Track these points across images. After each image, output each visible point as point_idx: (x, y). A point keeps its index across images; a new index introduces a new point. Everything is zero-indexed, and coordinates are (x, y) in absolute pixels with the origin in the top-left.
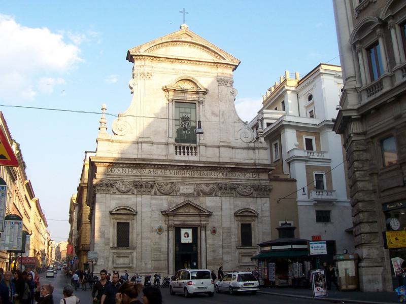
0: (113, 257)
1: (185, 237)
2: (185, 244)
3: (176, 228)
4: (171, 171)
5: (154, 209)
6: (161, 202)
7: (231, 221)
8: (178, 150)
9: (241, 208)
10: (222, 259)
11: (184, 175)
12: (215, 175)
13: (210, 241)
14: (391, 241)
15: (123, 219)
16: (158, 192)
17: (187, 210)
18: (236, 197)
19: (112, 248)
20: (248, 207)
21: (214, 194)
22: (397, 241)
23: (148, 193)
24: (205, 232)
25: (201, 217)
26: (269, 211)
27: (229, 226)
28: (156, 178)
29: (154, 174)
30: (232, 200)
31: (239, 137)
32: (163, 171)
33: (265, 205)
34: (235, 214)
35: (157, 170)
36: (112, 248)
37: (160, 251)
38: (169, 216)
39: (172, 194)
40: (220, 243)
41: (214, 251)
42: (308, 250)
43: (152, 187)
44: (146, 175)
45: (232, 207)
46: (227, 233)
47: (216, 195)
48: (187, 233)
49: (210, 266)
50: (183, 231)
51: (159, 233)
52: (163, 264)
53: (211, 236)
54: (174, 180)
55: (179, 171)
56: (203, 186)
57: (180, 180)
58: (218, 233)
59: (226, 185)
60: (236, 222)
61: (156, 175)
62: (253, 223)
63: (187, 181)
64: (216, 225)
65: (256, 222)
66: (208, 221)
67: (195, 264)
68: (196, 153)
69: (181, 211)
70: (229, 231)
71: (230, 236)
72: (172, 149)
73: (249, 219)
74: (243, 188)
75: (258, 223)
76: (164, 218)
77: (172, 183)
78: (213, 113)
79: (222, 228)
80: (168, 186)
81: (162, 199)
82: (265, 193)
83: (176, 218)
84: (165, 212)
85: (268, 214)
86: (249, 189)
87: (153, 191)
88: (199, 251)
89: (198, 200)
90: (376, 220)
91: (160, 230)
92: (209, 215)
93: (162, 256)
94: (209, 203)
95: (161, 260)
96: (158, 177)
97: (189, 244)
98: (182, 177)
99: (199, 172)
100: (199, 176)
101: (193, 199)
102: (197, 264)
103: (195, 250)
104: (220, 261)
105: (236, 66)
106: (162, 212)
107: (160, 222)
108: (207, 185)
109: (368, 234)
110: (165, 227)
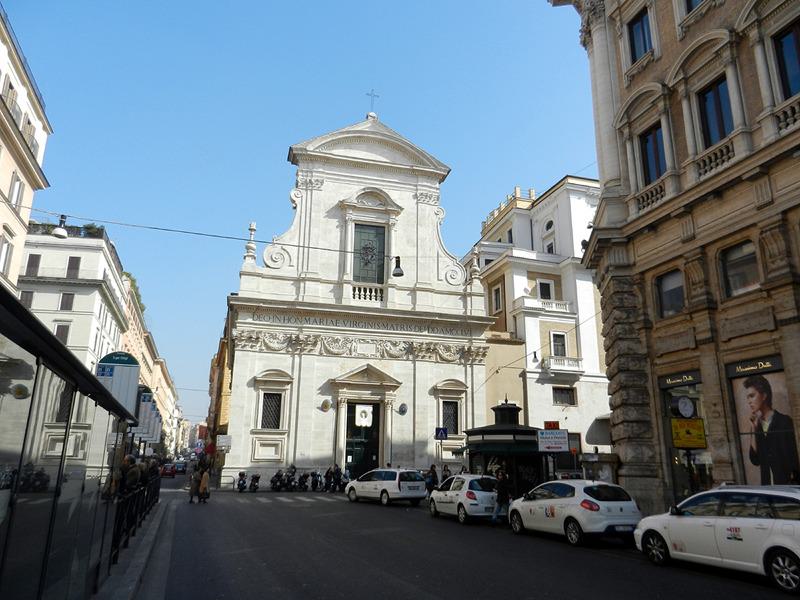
0: (253, 444)
8: (357, 292)
15: (273, 389)
19: (253, 432)
31: (442, 277)
36: (253, 432)
42: (535, 444)
43: (315, 344)
48: (364, 412)
50: (359, 409)
56: (389, 344)
67: (374, 458)
68: (382, 297)
72: (348, 290)
78: (408, 242)
91: (324, 407)
94: (395, 369)
102: (377, 458)
105: (444, 177)
108: (395, 344)
109: (635, 424)
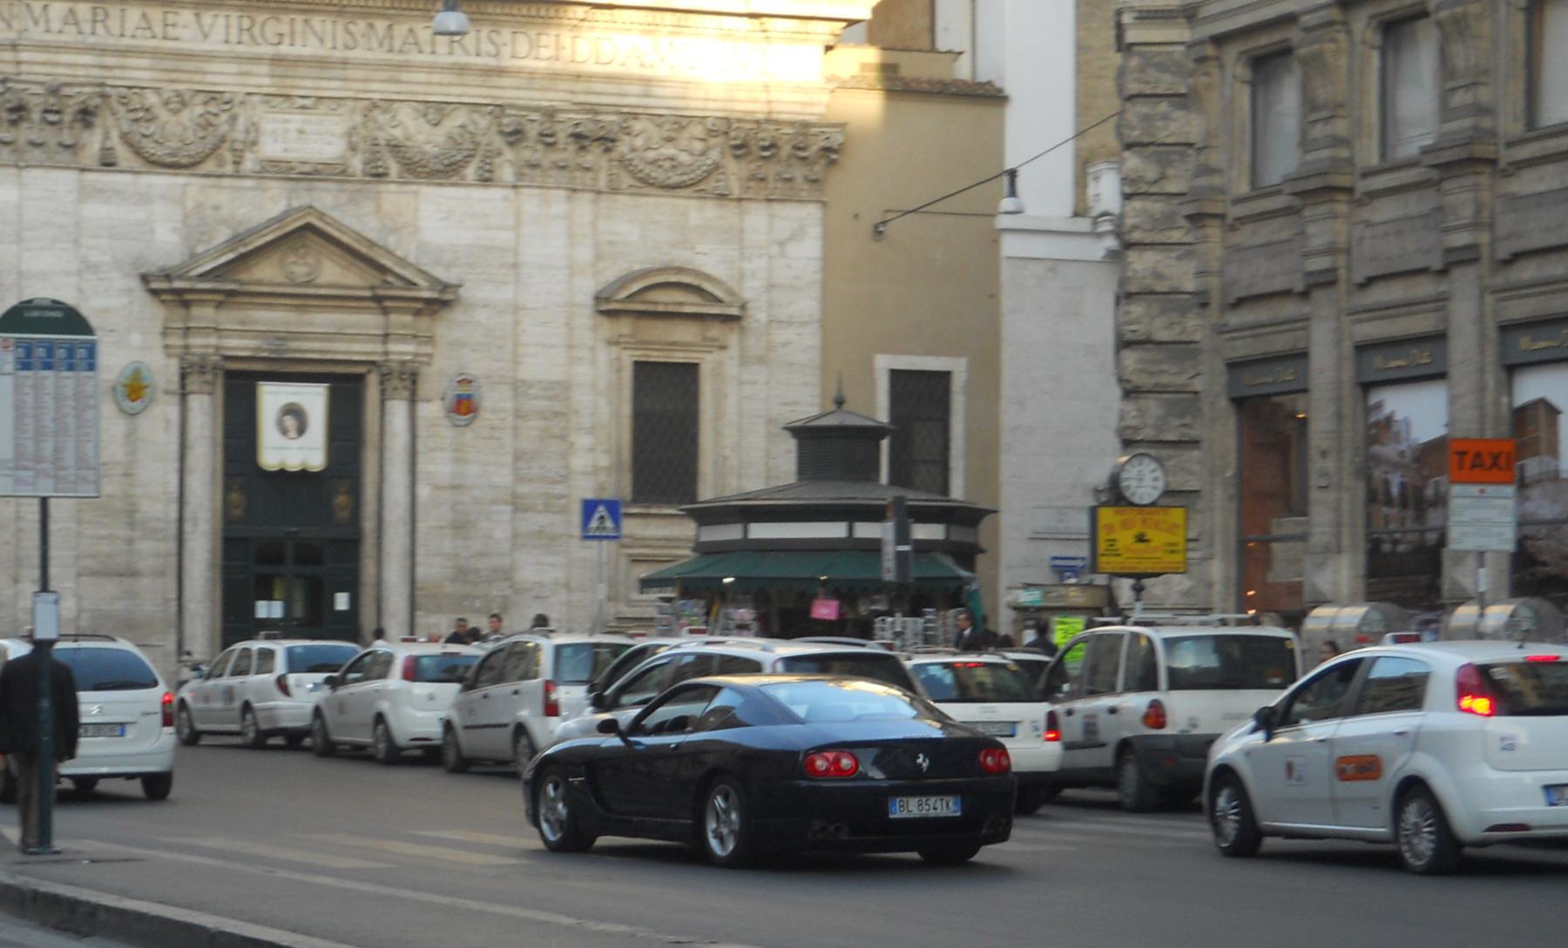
1: (284, 432)
2: (282, 474)
3: (230, 375)
4: (207, 18)
5: (95, 257)
6: (137, 214)
7: (571, 347)
9: (637, 267)
10: (507, 574)
11: (285, 49)
12: (486, 47)
13: (435, 466)
14: (1119, 545)
16: (123, 154)
17: (300, 271)
18: (614, 190)
20: (680, 256)
21: (470, 172)
22: (1142, 545)
23: (65, 156)
24: (413, 401)
25: (386, 311)
26: (816, 292)
27: (556, 375)
28: (110, 60)
29: (101, 38)
30: (584, 206)
32: (156, 14)
33: (794, 249)
34: (598, 299)
35: (114, 11)
37: (130, 514)
38: (186, 305)
39: (209, 166)
40: (503, 477)
41: (461, 526)
43: (86, 116)
44: (48, 37)
45: (584, 254)
46: (542, 415)
47: (486, 180)
49: (433, 619)
50: (272, 398)
51: (128, 405)
52: (152, 596)
53: (446, 432)
54: (223, 77)
55: (261, 18)
56: (406, 114)
57: (262, 79)
58: (486, 416)
59: (550, 113)
60: (604, 355)
61: (111, 41)
62: (708, 362)
63: (306, 85)
64: (477, 366)
65: (734, 351)
66: (430, 340)
67: (342, 601)
69: (266, 272)
70: (557, 406)
71: (563, 437)
73: (685, 332)
74: (656, 134)
75: (744, 361)
76: (156, 313)
77: (213, 96)
79: (519, 387)
80: (185, 116)
81: (145, 199)
82: (799, 172)
83: (229, 318)
84: (168, 277)
85: (807, 305)
86: (698, 146)
87: (93, 142)
88: (368, 525)
89: (368, 207)
90: (1193, 433)
92: (440, 301)
93: (144, 546)
95: (134, 574)
96: (125, 52)
97: (304, 474)
98: (276, 60)
99: (381, 25)
100: (381, 55)
101: (343, 198)
102: (355, 601)
103: (343, 515)
104: (498, 590)
106: (145, 278)
107: (136, 338)
108: (436, 111)
110: (163, 370)
